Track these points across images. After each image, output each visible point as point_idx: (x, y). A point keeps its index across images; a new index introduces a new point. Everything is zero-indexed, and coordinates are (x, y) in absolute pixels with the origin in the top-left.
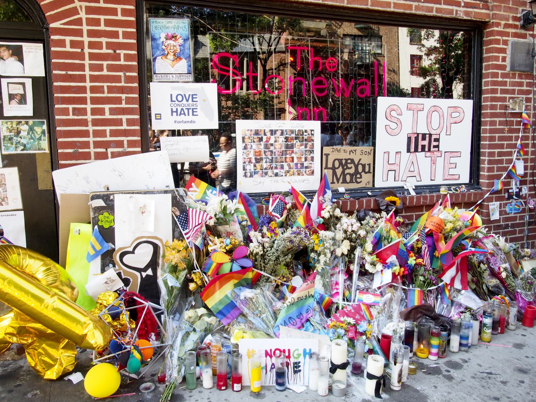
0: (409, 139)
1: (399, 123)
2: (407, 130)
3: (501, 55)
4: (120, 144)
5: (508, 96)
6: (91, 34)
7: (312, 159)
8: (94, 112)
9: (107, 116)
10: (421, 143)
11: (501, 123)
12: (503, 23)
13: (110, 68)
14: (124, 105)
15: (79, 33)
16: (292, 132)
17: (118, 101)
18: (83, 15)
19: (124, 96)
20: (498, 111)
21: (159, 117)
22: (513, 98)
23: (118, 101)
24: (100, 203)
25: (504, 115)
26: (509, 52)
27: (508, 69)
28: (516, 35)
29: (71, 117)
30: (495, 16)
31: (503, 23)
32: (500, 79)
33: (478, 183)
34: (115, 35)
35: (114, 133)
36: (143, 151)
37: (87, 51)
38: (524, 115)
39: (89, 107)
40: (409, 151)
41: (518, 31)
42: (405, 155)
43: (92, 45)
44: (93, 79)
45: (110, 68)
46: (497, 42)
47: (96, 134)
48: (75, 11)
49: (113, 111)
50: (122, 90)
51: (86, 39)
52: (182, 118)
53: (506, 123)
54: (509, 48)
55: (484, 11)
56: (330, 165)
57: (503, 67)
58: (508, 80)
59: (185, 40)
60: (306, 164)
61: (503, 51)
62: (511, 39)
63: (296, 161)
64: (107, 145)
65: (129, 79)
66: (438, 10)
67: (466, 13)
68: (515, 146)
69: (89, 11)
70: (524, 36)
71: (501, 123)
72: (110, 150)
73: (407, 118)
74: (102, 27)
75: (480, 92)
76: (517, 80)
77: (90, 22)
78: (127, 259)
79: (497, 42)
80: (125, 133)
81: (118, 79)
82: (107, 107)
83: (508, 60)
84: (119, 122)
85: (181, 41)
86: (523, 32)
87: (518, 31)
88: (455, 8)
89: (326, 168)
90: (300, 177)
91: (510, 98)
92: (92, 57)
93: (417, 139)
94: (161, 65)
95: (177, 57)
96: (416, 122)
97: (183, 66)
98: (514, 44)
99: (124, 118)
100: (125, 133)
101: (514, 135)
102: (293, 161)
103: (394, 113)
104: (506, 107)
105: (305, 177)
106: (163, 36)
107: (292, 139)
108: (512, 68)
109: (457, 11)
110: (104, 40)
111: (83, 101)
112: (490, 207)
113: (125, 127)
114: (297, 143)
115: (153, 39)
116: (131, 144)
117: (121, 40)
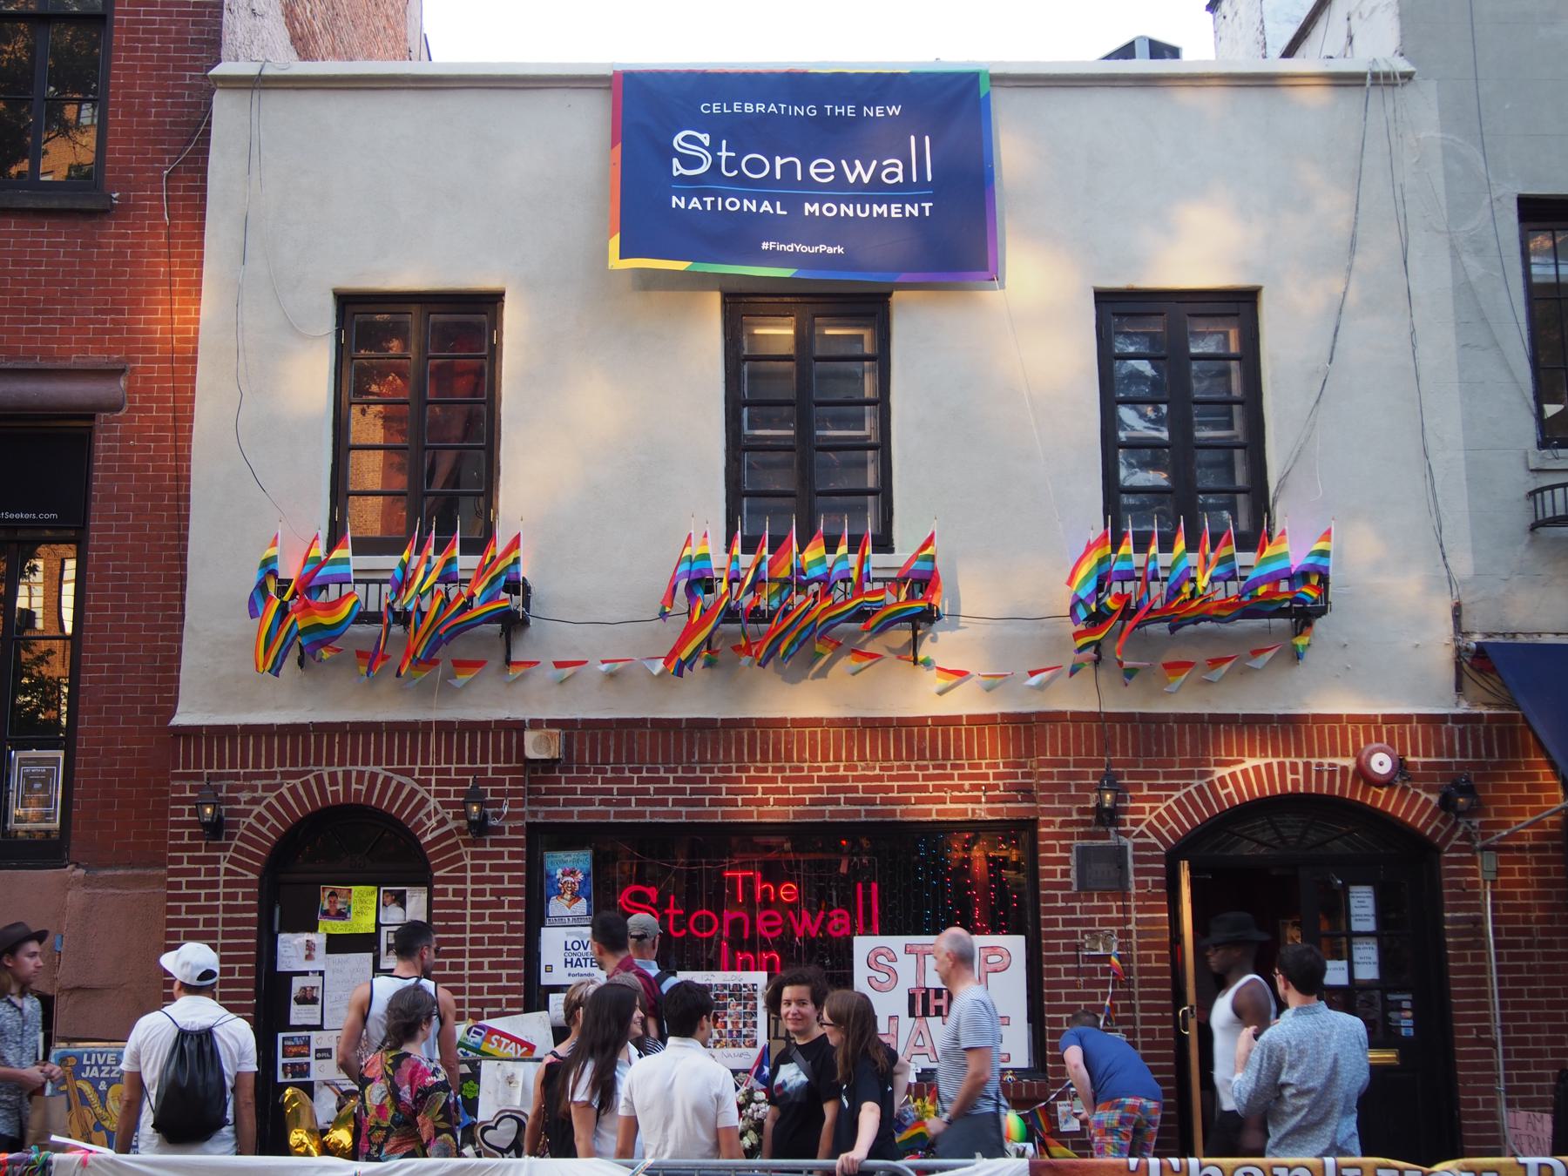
0: (912, 997)
1: (893, 974)
2: (907, 981)
3: (1059, 868)
4: (497, 1003)
5: (1079, 929)
6: (475, 880)
7: (755, 1024)
8: (472, 966)
9: (486, 971)
10: (934, 1002)
11: (1068, 972)
12: (1059, 819)
13: (492, 917)
14: (505, 958)
15: (463, 880)
16: (725, 986)
17: (499, 953)
18: (468, 861)
19: (505, 948)
20: (1062, 953)
21: (549, 969)
22: (1090, 932)
23: (499, 953)
24: (465, 1069)
25: (1075, 959)
26: (1073, 862)
27: (1075, 888)
28: (1083, 836)
29: (447, 972)
30: (1045, 812)
31: (1059, 819)
32: (1060, 904)
33: (1044, 1069)
34: (500, 880)
35: (491, 990)
36: (526, 1011)
37: (469, 898)
38: (1114, 959)
39: (467, 960)
40: (912, 1014)
41: (1091, 829)
42: (906, 1023)
43: (475, 893)
44: (474, 929)
45: (492, 917)
46: (1052, 849)
47: (473, 991)
48: (460, 858)
49: (492, 965)
50: (504, 941)
51: (469, 887)
52: (579, 970)
53: (1078, 972)
54: (1073, 856)
55: (1025, 805)
56: (782, 1033)
57: (1067, 886)
58: (1078, 905)
59: (586, 876)
60: (744, 1031)
61: (1065, 861)
62: (1076, 842)
63: (730, 1026)
64: (482, 1004)
65: (512, 929)
66: (939, 812)
67: (990, 811)
68: (1101, 1008)
69: (475, 856)
70: (1106, 836)
71: (1068, 972)
72: (486, 1010)
73: (906, 967)
74: (487, 873)
75: (1037, 923)
76: (1096, 903)
77: (475, 868)
78: (489, 1135)
79: (1052, 849)
80: (504, 990)
81: (499, 929)
82: (486, 960)
83: (1073, 874)
84: (498, 978)
85: (580, 877)
86: (1102, 829)
87: (1091, 829)
88: (970, 806)
89: (776, 1037)
90: (737, 1050)
91: (1083, 933)
92: (475, 905)
93: (925, 997)
94: (557, 907)
95: (576, 897)
96: (921, 970)
97: (582, 906)
98: (1082, 851)
99: (504, 972)
100: (504, 990)
101: (1099, 991)
102: (725, 1026)
103: (881, 959)
104: (1077, 947)
105: (744, 1050)
106: (559, 872)
107: (725, 996)
108: (1080, 888)
109: (973, 810)
110: (488, 887)
111: (461, 954)
112: (1060, 1109)
113: (504, 983)
114: (731, 1001)
115: (549, 877)
116: (510, 1003)
117: (506, 885)
